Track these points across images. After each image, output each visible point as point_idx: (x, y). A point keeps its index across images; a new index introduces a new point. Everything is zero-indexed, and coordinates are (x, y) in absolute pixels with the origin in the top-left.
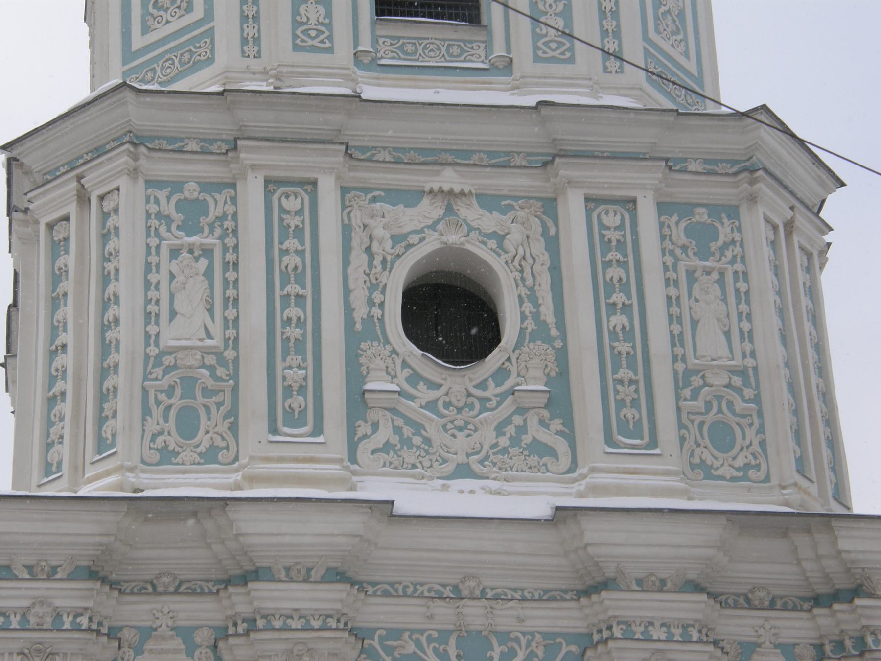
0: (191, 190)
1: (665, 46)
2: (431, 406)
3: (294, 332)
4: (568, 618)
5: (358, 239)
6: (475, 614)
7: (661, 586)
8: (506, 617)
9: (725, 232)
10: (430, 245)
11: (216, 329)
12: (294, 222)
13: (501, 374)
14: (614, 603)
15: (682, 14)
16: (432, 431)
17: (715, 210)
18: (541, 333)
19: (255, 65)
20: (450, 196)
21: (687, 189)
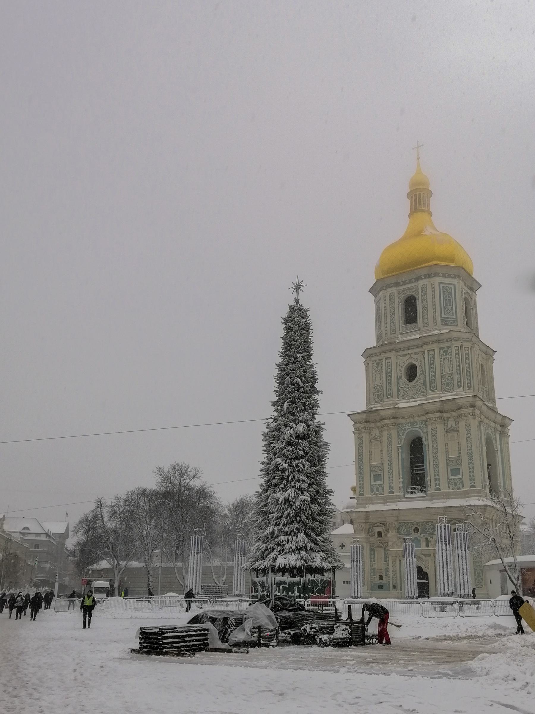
0: (378, 361)
1: (446, 316)
2: (408, 388)
3: (389, 381)
4: (424, 418)
5: (398, 363)
6: (412, 420)
7: (434, 412)
8: (416, 419)
9: (449, 351)
10: (408, 363)
11: (381, 382)
12: (389, 364)
13: (417, 382)
14: (428, 416)
15: (452, 309)
16: (409, 393)
17: (448, 347)
18: (423, 374)
19: (387, 338)
20: (410, 354)
21: (442, 345)
